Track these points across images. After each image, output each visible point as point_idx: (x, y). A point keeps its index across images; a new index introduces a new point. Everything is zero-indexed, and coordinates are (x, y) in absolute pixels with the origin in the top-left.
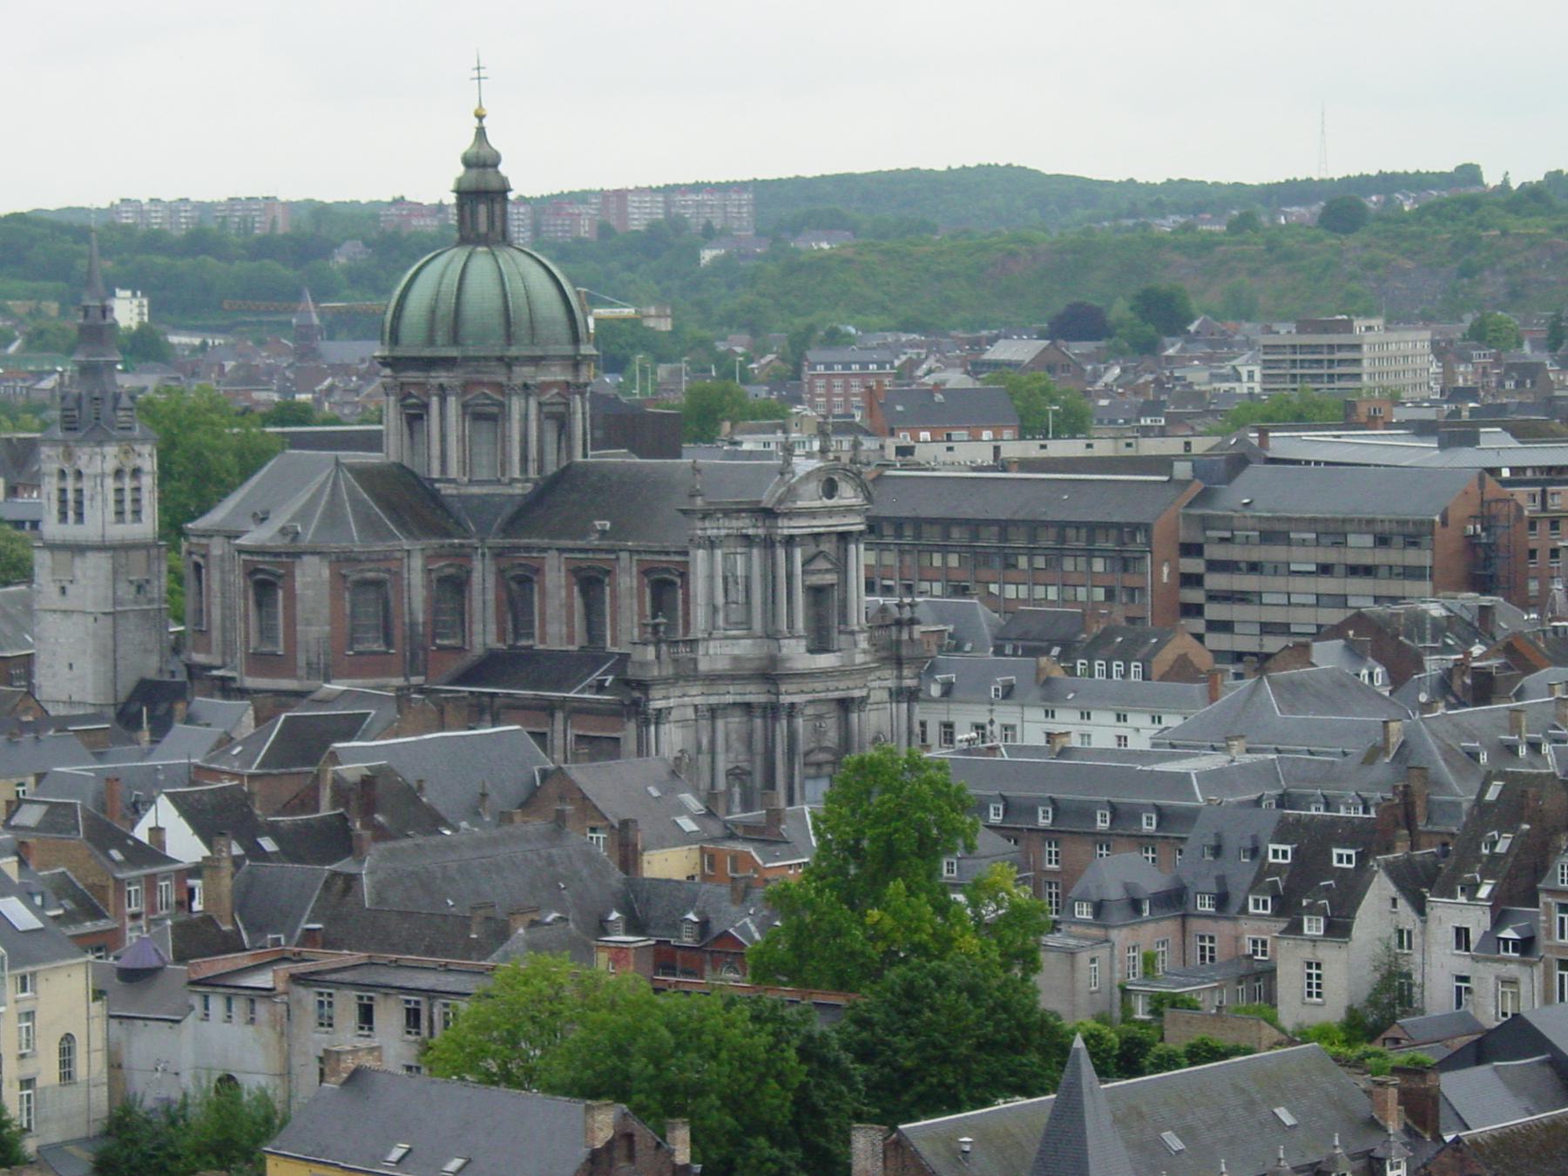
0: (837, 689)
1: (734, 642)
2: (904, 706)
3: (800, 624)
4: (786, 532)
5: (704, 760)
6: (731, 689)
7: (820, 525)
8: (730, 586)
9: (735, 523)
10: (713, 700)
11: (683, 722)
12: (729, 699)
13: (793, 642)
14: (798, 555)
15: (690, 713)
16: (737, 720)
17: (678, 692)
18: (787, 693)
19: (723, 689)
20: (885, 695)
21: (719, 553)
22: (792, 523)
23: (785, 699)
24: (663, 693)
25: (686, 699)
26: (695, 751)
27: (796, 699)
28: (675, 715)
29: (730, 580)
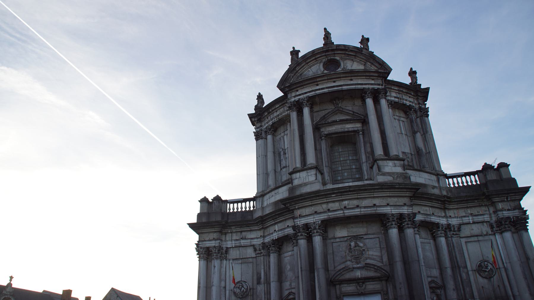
0: (358, 206)
1: (276, 191)
2: (508, 235)
3: (311, 159)
4: (293, 99)
5: (261, 288)
6: (276, 227)
7: (324, 87)
8: (282, 157)
9: (275, 114)
10: (267, 240)
11: (243, 260)
12: (275, 236)
13: (303, 174)
14: (306, 111)
15: (250, 252)
16: (290, 253)
17: (235, 237)
18: (301, 216)
19: (271, 229)
20: (485, 229)
21: (269, 137)
22: (298, 93)
23: (301, 222)
24: (215, 235)
25: (242, 241)
26: (255, 282)
27: (310, 220)
28: (233, 254)
29: (282, 153)
